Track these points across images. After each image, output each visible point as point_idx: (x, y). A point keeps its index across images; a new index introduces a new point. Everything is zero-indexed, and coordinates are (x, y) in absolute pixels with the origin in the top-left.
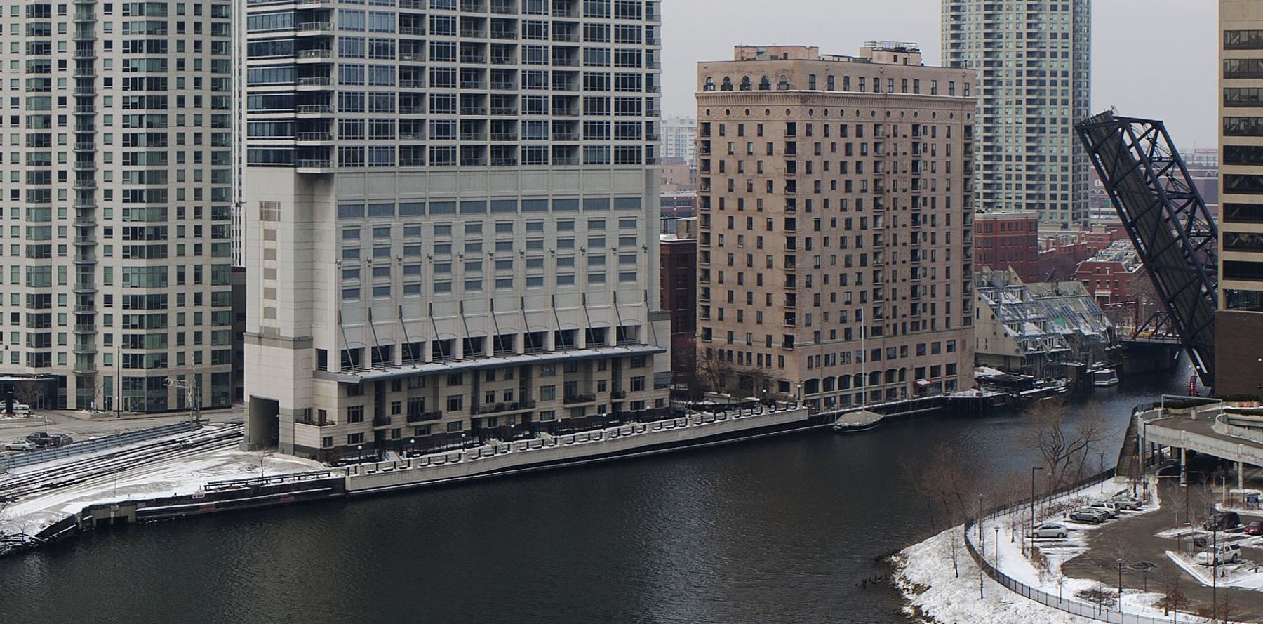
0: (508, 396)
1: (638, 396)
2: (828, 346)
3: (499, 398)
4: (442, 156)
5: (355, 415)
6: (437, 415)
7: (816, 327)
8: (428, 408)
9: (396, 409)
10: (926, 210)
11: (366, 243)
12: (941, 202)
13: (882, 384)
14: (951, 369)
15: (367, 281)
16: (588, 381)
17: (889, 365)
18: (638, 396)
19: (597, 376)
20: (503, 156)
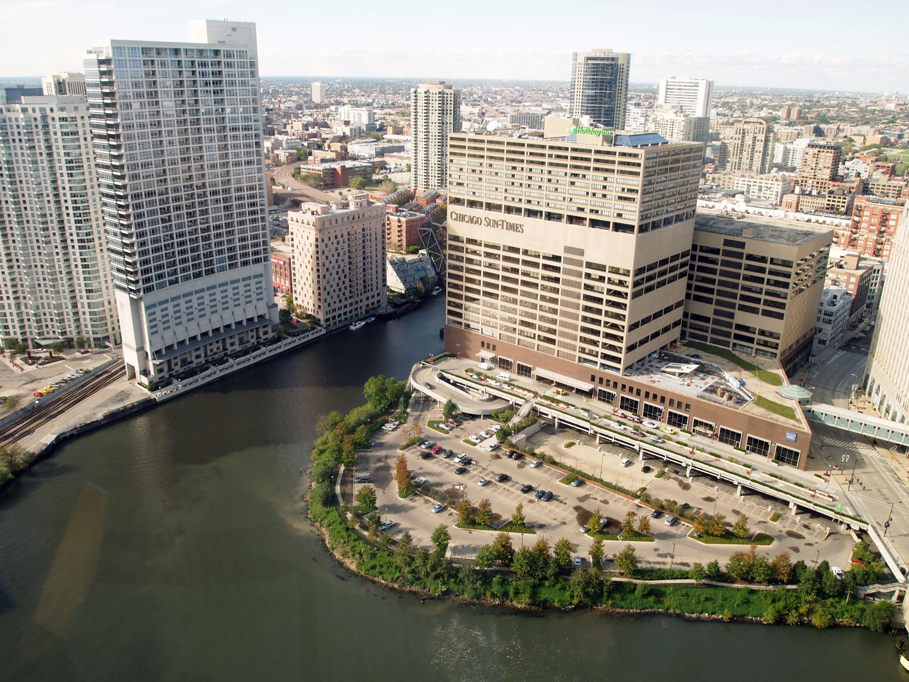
0: (218, 348)
1: (266, 336)
2: (333, 306)
3: (215, 350)
5: (160, 371)
6: (191, 362)
9: (176, 364)
11: (159, 315)
14: (378, 302)
15: (161, 326)
18: (266, 336)
20: (211, 272)
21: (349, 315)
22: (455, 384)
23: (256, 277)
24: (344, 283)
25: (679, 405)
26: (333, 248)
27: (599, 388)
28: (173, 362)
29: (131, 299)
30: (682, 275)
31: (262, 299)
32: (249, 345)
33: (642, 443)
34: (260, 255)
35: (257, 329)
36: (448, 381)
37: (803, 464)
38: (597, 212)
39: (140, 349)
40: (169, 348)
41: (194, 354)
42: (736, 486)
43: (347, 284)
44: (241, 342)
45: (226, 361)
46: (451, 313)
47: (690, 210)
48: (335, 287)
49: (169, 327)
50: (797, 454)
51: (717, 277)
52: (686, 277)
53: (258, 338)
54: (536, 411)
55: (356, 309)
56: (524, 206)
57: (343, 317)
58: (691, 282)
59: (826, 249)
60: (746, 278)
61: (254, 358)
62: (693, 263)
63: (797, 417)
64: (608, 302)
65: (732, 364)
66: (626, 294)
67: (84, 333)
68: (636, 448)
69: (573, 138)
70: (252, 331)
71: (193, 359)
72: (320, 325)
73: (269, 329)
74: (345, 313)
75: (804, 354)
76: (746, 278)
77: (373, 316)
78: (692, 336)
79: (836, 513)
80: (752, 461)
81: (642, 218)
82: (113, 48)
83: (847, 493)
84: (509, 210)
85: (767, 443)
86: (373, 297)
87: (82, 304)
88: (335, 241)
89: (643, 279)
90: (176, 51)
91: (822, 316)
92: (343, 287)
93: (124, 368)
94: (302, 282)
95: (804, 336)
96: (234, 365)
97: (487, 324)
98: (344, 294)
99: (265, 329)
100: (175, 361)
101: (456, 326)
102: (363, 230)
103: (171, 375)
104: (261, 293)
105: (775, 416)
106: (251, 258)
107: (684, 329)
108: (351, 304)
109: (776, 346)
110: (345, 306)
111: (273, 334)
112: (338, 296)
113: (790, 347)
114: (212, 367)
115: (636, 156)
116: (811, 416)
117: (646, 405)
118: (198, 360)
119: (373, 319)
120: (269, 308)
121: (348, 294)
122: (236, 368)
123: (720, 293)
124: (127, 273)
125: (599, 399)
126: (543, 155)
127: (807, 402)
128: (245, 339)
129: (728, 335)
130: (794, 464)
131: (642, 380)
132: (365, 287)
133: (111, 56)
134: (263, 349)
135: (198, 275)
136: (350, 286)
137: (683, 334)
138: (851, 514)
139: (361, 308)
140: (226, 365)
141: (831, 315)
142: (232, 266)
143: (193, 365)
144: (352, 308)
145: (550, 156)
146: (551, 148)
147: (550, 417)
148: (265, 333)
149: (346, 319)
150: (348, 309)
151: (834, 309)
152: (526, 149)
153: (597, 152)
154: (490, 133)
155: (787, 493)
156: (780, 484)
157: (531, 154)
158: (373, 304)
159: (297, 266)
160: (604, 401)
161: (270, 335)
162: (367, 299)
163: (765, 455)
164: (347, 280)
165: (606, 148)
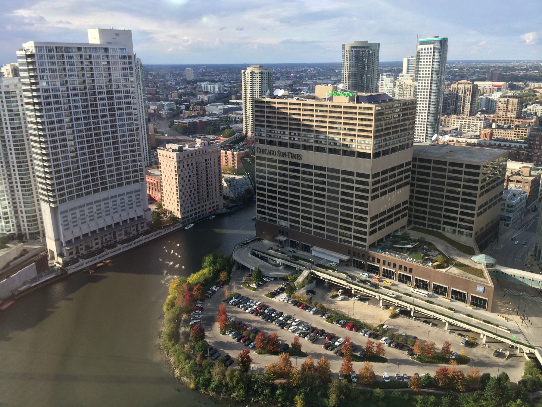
0: (111, 238)
1: (143, 229)
2: (187, 209)
4: (88, 194)
5: (71, 254)
6: (92, 247)
7: (183, 199)
8: (90, 246)
9: (82, 249)
10: (209, 162)
11: (70, 218)
12: (212, 159)
13: (201, 213)
14: (217, 205)
16: (130, 229)
17: (202, 209)
18: (143, 229)
19: (132, 228)
21: (198, 215)
22: (262, 258)
23: (135, 192)
24: (194, 194)
25: (405, 269)
26: (186, 172)
28: (80, 247)
29: (51, 207)
30: (406, 184)
31: (140, 205)
32: (132, 235)
33: (381, 295)
34: (138, 177)
35: (137, 225)
36: (257, 256)
37: (490, 307)
38: (347, 145)
39: (57, 240)
40: (77, 238)
41: (94, 242)
42: (444, 324)
43: (196, 195)
44: (127, 233)
45: (116, 246)
46: (259, 212)
47: (410, 142)
48: (188, 197)
49: (77, 225)
50: (485, 301)
51: (430, 185)
53: (137, 230)
55: (202, 211)
56: (301, 143)
57: (194, 216)
59: (504, 163)
60: (448, 184)
61: (135, 243)
62: (414, 176)
67: (22, 230)
68: (377, 297)
69: (330, 99)
70: (133, 226)
71: (94, 245)
72: (178, 221)
73: (145, 225)
74: (195, 214)
76: (448, 184)
77: (213, 215)
78: (415, 223)
79: (513, 341)
81: (374, 150)
82: (36, 47)
83: (521, 327)
84: (293, 146)
86: (213, 203)
87: (21, 211)
88: (187, 168)
89: (378, 187)
90: (79, 49)
91: (506, 207)
92: (193, 197)
93: (47, 252)
94: (167, 194)
95: (492, 221)
96: (121, 249)
97: (281, 218)
98: (194, 201)
99: (143, 225)
100: (81, 247)
101: (263, 220)
102: (206, 160)
103: (78, 256)
104: (140, 202)
105: (470, 275)
106: (132, 180)
107: (410, 219)
108: (199, 208)
109: (471, 229)
110: (195, 209)
111: (148, 228)
112: (190, 203)
113: (482, 229)
114: (106, 250)
115: (370, 109)
118: (97, 246)
119: (213, 217)
120: (145, 211)
121: (197, 201)
122: (122, 250)
123: (432, 195)
124: (48, 190)
125: (354, 266)
126: (312, 110)
127: (493, 266)
128: (129, 231)
130: (484, 308)
132: (208, 196)
133: (34, 51)
134: (141, 238)
135: (95, 191)
136: (198, 196)
137: (409, 222)
138: (524, 342)
139: (206, 210)
140: (116, 248)
141: (512, 206)
142: (119, 185)
143: (94, 249)
144: (200, 210)
145: (316, 111)
146: (317, 105)
147: (321, 278)
148: (142, 227)
149: (196, 217)
150: (197, 211)
151: (514, 202)
152: (301, 107)
153: (345, 107)
154: (280, 97)
156: (474, 321)
157: (305, 110)
158: (213, 207)
159: (164, 184)
160: (357, 267)
161: (146, 228)
162: (210, 204)
163: (464, 301)
164: (196, 193)
165: (352, 105)
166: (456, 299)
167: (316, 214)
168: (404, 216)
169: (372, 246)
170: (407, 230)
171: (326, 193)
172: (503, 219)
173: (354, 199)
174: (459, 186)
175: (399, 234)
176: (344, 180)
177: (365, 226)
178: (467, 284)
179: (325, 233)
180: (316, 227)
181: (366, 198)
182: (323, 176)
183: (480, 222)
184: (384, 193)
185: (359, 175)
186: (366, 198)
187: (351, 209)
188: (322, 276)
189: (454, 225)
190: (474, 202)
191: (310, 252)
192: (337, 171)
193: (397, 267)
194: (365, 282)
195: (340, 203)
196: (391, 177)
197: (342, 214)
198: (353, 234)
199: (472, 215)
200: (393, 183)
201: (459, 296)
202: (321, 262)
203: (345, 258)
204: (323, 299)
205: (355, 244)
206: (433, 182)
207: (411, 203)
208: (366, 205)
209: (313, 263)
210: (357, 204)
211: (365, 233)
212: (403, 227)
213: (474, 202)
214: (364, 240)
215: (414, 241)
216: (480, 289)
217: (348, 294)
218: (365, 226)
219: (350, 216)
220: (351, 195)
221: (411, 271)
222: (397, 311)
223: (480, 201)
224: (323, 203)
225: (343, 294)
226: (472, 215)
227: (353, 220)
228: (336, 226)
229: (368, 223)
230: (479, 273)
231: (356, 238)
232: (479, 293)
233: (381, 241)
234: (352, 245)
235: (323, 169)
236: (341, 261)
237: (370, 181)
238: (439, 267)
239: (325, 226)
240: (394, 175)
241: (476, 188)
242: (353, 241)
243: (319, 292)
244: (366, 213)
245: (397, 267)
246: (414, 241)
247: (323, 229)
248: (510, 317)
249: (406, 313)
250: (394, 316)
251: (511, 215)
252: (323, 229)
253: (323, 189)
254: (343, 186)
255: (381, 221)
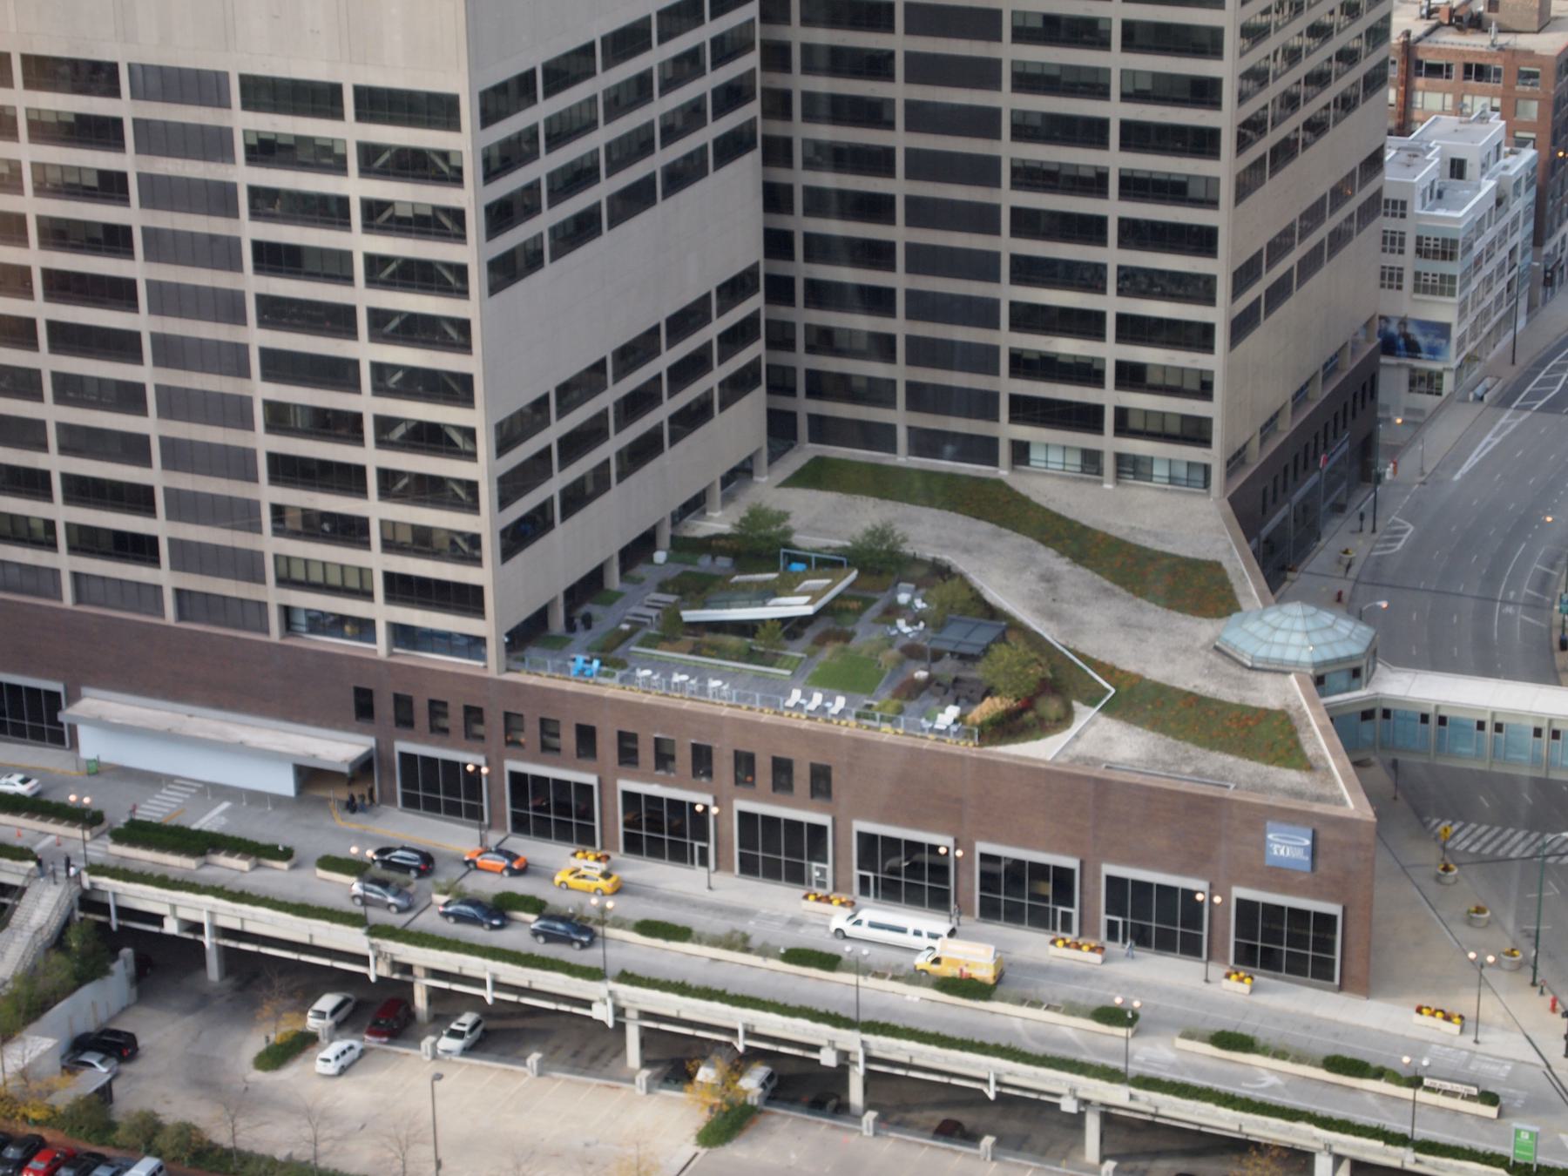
27: (402, 746)
30: (731, 147)
33: (626, 992)
42: (1076, 1122)
50: (1326, 921)
52: (753, 158)
54: (103, 908)
58: (780, 175)
60: (1025, 130)
63: (1309, 750)
64: (379, 318)
65: (1014, 540)
66: (461, 271)
68: (602, 1013)
75: (1343, 447)
76: (1025, 130)
78: (823, 429)
80: (1131, 986)
85: (1189, 894)
89: (532, 188)
91: (1408, 262)
95: (1330, 367)
107: (784, 403)
113: (1269, 426)
116: (1370, 733)
117: (631, 799)
125: (410, 802)
129: (985, 405)
131: (570, 679)
137: (781, 429)
141: (1446, 250)
147: (171, 927)
151: (1456, 216)
155: (1293, 1115)
156: (1263, 1074)
160: (432, 807)
163: (1191, 948)
166: (1141, 938)
167: (77, 441)
168: (738, 385)
169: (528, 635)
170: (766, 490)
171: (136, 269)
172: (1397, 342)
173: (362, 297)
174: (1092, 132)
175: (718, 522)
176: (265, 151)
177: (464, 496)
178: (1199, 821)
179: (164, 577)
180: (86, 541)
181: (448, 280)
182: (104, 132)
183: (1249, 384)
184: (582, 229)
185: (378, 104)
186: (448, 280)
187: (341, 374)
188: (176, 909)
189: (1087, 418)
190: (1203, 241)
191: (59, 736)
192: (202, 86)
193: (724, 766)
194: (499, 910)
195: (257, 337)
196: (618, 103)
197: (279, 417)
198: (377, 561)
199: (1200, 337)
200: (639, 145)
201: (1158, 921)
202: (155, 809)
203: (339, 748)
204: (206, 1082)
205: (404, 635)
206: (922, 117)
207: (780, 290)
208: (456, 335)
209: (88, 819)
210: (385, 326)
211: (466, 548)
212: (740, 474)
213: (1203, 241)
214: (467, 599)
215: (828, 563)
216: (1287, 847)
217: (384, 1012)
218: (464, 496)
219: (345, 426)
220: (335, 267)
221: (821, 783)
222: (752, 1083)
223: (1239, 228)
224: (123, 346)
225: (346, 1021)
226: (1200, 337)
227: (370, 456)
228: (243, 515)
229: (482, 470)
230: (1270, 736)
231: (402, 588)
232: (1279, 877)
233: (589, 588)
234: (381, 647)
235: (96, 76)
236: (310, 777)
237: (464, 143)
238: (1007, 727)
239: (159, 526)
240: (640, 90)
241: (1203, 143)
242: (382, 612)
243: (163, 1033)
244: (457, 389)
245: (724, 766)
246: (828, 563)
247: (141, 549)
248: (1491, 1007)
249: (805, 1086)
250: (729, 1124)
251: (1442, 310)
252: (141, 549)
253: (115, 240)
254: (265, 202)
255: (574, 445)
